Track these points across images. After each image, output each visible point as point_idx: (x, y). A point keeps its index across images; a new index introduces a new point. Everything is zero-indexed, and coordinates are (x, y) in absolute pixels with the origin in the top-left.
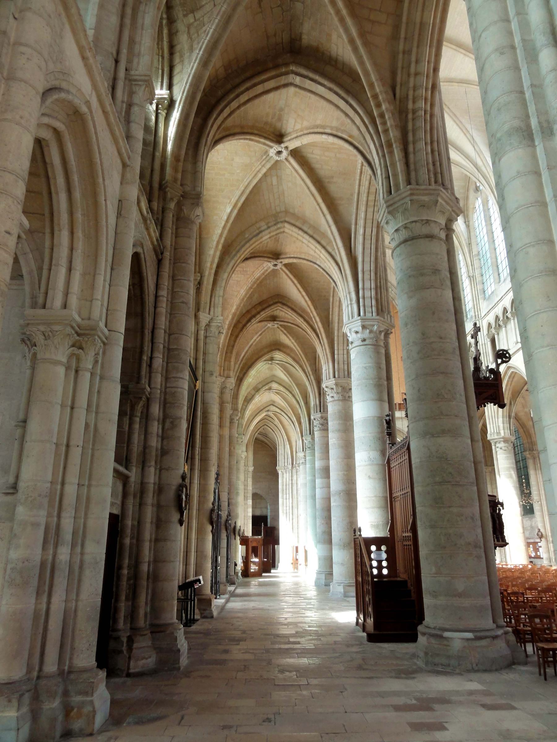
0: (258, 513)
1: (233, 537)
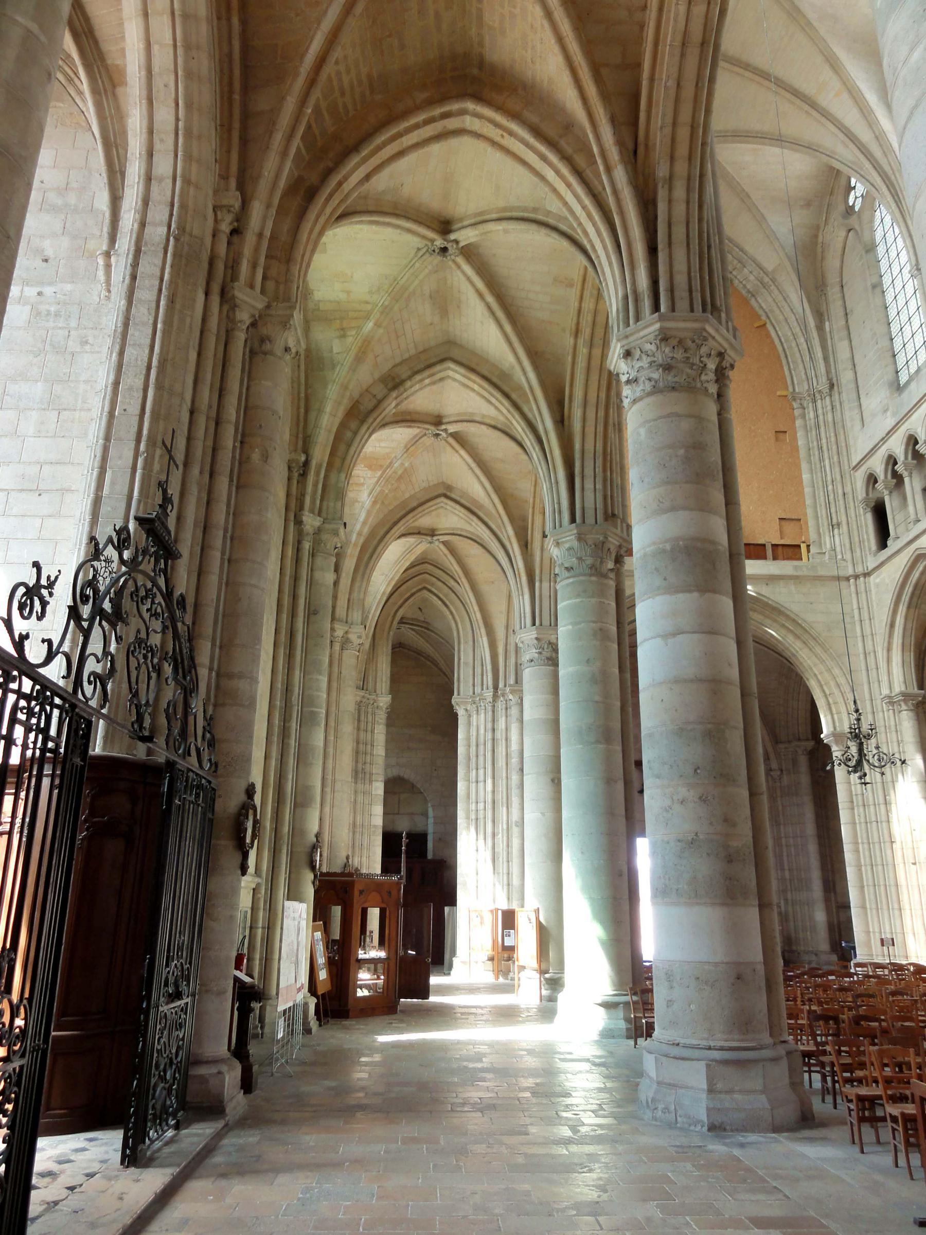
0: (403, 826)
1: (231, 859)
